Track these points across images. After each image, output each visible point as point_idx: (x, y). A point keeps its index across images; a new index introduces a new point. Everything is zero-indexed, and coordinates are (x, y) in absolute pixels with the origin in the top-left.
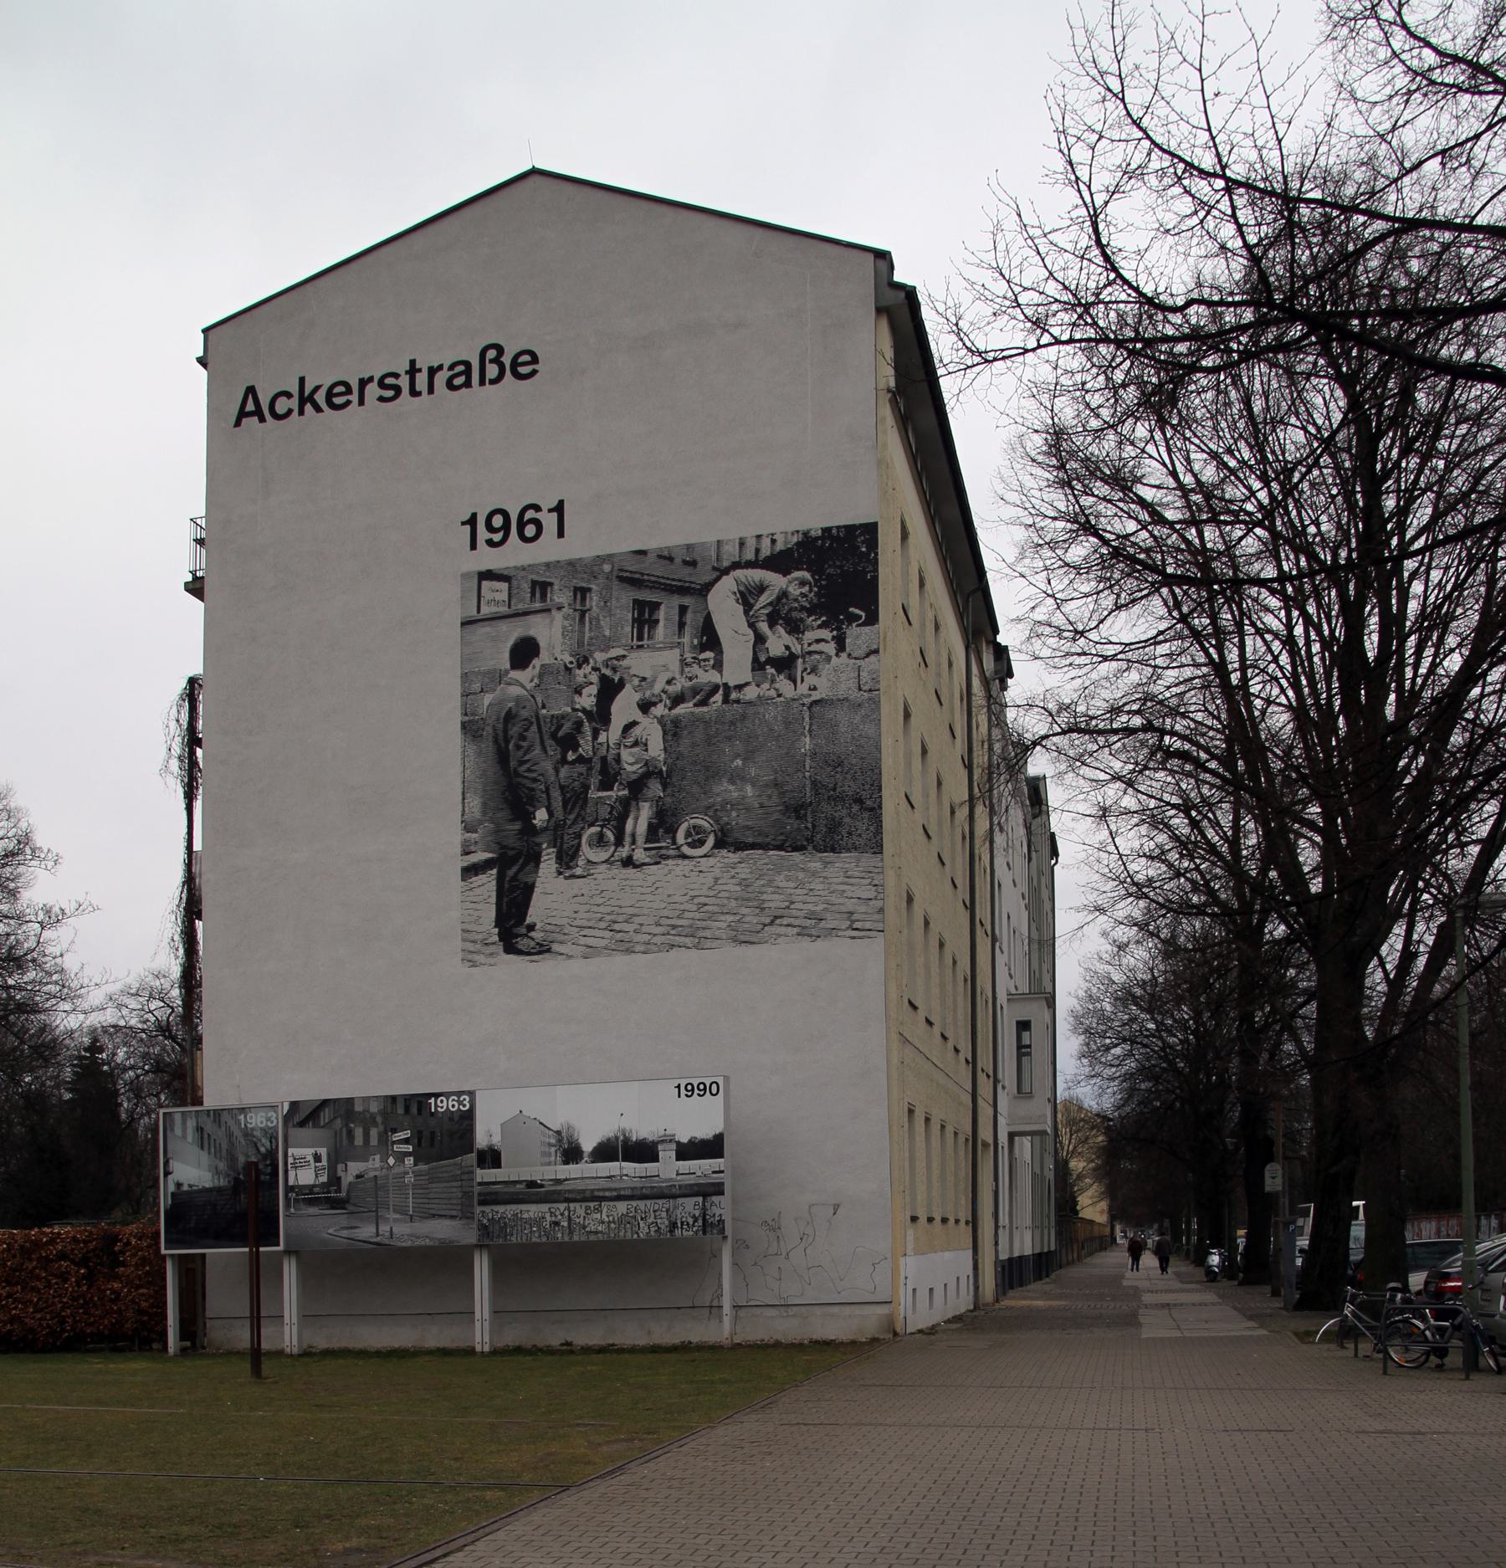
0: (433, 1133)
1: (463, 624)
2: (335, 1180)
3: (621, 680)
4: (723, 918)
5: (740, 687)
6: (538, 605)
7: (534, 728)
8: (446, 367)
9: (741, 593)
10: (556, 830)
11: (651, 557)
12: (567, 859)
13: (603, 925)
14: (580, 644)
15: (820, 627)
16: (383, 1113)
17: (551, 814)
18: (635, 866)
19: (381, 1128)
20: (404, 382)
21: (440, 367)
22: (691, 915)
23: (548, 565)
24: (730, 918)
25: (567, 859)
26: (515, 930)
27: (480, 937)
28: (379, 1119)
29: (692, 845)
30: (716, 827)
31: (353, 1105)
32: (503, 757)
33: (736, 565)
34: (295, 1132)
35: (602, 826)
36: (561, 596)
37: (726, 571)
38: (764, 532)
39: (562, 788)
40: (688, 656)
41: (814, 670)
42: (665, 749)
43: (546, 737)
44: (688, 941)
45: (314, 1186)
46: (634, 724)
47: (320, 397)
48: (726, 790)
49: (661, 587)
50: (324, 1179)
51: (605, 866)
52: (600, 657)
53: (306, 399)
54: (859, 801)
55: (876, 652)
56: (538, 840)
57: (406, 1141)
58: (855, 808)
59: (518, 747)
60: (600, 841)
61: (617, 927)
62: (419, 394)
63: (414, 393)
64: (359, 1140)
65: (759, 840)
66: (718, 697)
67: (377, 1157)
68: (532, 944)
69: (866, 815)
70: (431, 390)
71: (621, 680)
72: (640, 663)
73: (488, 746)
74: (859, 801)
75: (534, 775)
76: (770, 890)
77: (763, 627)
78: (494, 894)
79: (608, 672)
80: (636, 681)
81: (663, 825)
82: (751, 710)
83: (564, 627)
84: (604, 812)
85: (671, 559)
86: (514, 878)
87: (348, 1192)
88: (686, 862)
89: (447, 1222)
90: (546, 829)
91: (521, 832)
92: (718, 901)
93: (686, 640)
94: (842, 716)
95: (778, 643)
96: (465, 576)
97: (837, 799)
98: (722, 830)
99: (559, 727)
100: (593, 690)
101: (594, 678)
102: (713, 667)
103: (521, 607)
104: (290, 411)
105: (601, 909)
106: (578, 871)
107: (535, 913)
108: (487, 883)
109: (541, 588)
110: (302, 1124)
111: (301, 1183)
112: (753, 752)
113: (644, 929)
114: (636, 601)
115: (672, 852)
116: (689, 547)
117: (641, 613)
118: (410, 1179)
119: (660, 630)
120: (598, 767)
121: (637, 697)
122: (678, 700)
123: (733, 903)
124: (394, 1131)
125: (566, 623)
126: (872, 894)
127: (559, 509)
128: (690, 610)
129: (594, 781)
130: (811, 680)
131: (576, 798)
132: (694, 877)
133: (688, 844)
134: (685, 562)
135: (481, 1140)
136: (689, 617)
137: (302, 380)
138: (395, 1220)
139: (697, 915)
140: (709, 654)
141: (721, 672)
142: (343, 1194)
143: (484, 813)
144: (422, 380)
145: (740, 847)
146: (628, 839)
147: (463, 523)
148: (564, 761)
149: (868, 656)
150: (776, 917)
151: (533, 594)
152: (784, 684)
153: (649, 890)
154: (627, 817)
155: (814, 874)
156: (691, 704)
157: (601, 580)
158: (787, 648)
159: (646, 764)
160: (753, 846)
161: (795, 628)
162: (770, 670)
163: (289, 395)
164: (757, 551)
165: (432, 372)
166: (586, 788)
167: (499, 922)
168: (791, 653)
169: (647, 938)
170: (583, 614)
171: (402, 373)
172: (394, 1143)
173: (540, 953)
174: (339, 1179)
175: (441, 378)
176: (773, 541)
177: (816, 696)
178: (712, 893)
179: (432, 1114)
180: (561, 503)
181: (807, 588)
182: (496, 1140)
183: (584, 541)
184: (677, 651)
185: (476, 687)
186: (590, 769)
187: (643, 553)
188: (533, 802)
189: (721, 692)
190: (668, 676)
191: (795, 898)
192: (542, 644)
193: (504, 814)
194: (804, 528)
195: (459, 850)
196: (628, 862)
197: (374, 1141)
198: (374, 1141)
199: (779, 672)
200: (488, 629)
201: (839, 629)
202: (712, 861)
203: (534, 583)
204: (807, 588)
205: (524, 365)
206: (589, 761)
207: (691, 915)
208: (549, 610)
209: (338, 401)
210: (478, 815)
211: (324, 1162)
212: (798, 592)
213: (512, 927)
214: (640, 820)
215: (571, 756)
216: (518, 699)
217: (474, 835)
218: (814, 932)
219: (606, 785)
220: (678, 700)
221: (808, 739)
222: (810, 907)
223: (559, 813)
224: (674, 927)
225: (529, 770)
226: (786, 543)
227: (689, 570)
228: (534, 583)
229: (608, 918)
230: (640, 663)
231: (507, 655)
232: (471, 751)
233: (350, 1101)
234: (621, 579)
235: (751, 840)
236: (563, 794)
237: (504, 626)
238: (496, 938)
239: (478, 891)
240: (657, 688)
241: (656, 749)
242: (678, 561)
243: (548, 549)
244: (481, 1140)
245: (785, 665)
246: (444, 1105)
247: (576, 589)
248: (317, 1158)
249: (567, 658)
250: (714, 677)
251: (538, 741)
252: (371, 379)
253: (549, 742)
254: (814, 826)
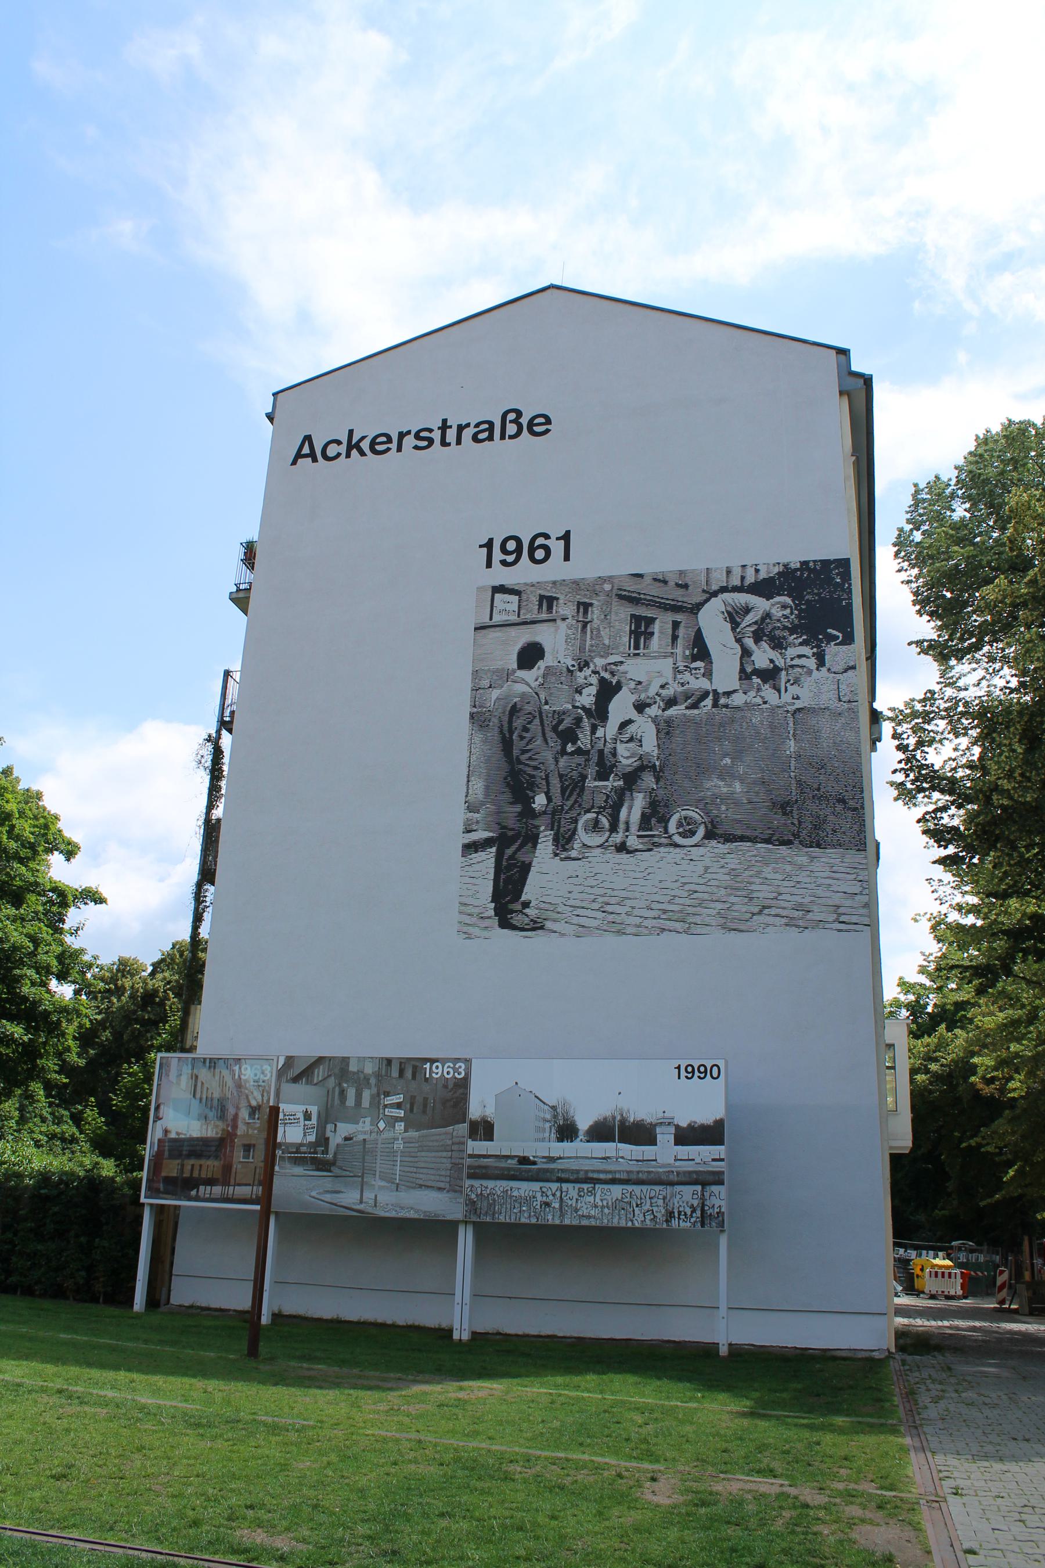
0: (426, 1099)
1: (476, 629)
2: (323, 1141)
3: (619, 683)
4: (712, 905)
5: (728, 694)
6: (544, 616)
7: (537, 721)
8: (472, 425)
9: (729, 613)
10: (554, 814)
11: (648, 580)
12: (563, 842)
13: (596, 906)
14: (582, 649)
15: (801, 644)
16: (378, 1075)
17: (549, 799)
18: (629, 852)
19: (374, 1090)
20: (436, 435)
21: (468, 425)
22: (681, 901)
23: (554, 583)
24: (719, 906)
25: (563, 842)
26: (511, 906)
27: (477, 910)
28: (373, 1081)
29: (683, 835)
30: (706, 819)
31: (348, 1065)
32: (507, 745)
33: (724, 590)
34: (288, 1088)
35: (598, 813)
36: (565, 608)
37: (715, 594)
38: (749, 563)
39: (561, 776)
40: (681, 665)
41: (796, 682)
42: (659, 745)
43: (548, 729)
44: (678, 926)
45: (302, 1145)
46: (630, 722)
47: (365, 445)
48: (715, 785)
49: (655, 607)
50: (312, 1138)
51: (599, 850)
52: (599, 662)
53: (353, 446)
54: (842, 801)
55: (853, 668)
56: (536, 822)
57: (399, 1106)
58: (839, 807)
59: (522, 738)
60: (596, 826)
61: (609, 908)
62: (449, 444)
63: (444, 443)
64: (350, 1101)
65: (748, 833)
66: (708, 702)
67: (368, 1120)
68: (527, 920)
69: (850, 814)
70: (459, 442)
71: (619, 683)
72: (635, 669)
73: (494, 734)
74: (842, 801)
75: (532, 763)
76: (758, 881)
77: (749, 642)
78: (492, 871)
79: (607, 676)
80: (632, 685)
81: (655, 815)
82: (738, 715)
83: (567, 636)
84: (600, 800)
85: (665, 582)
86: (512, 857)
87: (335, 1154)
88: (678, 850)
89: (434, 1194)
90: (545, 813)
91: (521, 815)
92: (708, 889)
93: (679, 650)
94: (825, 726)
95: (763, 656)
96: (480, 589)
97: (821, 799)
98: (712, 822)
99: (561, 722)
100: (593, 690)
101: (594, 680)
102: (704, 676)
103: (529, 617)
104: (339, 455)
105: (596, 891)
106: (574, 854)
107: (530, 892)
108: (487, 859)
109: (548, 602)
110: (296, 1080)
111: (289, 1140)
112: (741, 752)
113: (636, 912)
114: (633, 616)
115: (663, 841)
116: (681, 573)
117: (638, 626)
118: (399, 1145)
119: (655, 642)
120: (595, 759)
121: (633, 698)
122: (671, 702)
123: (723, 892)
124: (387, 1094)
125: (569, 632)
126: (857, 890)
127: (566, 537)
128: (682, 625)
129: (591, 771)
130: (793, 690)
131: (574, 786)
132: (682, 866)
133: (680, 834)
134: (677, 585)
135: (475, 1112)
136: (681, 632)
137: (351, 432)
138: (381, 1188)
139: (688, 902)
140: (699, 664)
141: (710, 680)
142: (330, 1156)
143: (487, 794)
144: (451, 435)
145: (729, 838)
146: (622, 826)
147: (481, 546)
148: (563, 752)
149: (846, 671)
150: (764, 907)
151: (540, 605)
152: (768, 692)
153: (641, 875)
154: (622, 805)
155: (801, 867)
156: (683, 707)
157: (602, 597)
158: (772, 661)
159: (640, 758)
160: (742, 839)
161: (778, 644)
162: (756, 680)
163: (339, 443)
164: (743, 578)
165: (461, 428)
166: (584, 777)
167: (496, 897)
168: (775, 666)
169: (638, 920)
170: (584, 627)
171: (436, 429)
172: (386, 1106)
173: (533, 929)
174: (328, 1139)
175: (468, 434)
176: (757, 571)
177: (799, 704)
178: (702, 881)
179: (426, 1080)
180: (568, 533)
181: (788, 611)
182: (490, 1112)
183: (585, 566)
184: (670, 660)
185: (485, 683)
186: (587, 760)
187: (640, 576)
188: (532, 786)
189: (711, 697)
190: (662, 681)
191: (782, 890)
192: (547, 649)
193: (508, 796)
194: (786, 561)
195: (461, 828)
196: (622, 848)
197: (366, 1102)
198: (366, 1102)
199: (765, 682)
200: (499, 634)
201: (818, 646)
202: (701, 850)
203: (542, 598)
204: (788, 611)
205: (538, 426)
206: (587, 752)
207: (681, 901)
208: (555, 620)
210: (481, 797)
211: (314, 1120)
212: (780, 614)
213: (508, 901)
214: (634, 809)
215: (570, 748)
216: (523, 695)
217: (476, 815)
218: (801, 923)
219: (602, 776)
220: (671, 702)
221: (792, 743)
222: (798, 899)
223: (557, 800)
224: (665, 911)
225: (530, 758)
226: (768, 572)
227: (681, 591)
228: (542, 598)
229: (600, 900)
230: (635, 669)
231: (515, 657)
232: (478, 738)
233: (345, 1060)
234: (621, 597)
235: (739, 833)
236: (561, 781)
237: (513, 631)
238: (492, 913)
239: (476, 867)
240: (652, 692)
241: (650, 745)
242: (672, 583)
243: (555, 570)
244: (475, 1112)
245: (769, 675)
246: (438, 1072)
247: (579, 604)
248: (307, 1116)
249: (570, 662)
250: (704, 684)
251: (540, 734)
252: (409, 433)
253: (550, 734)
254: (800, 822)
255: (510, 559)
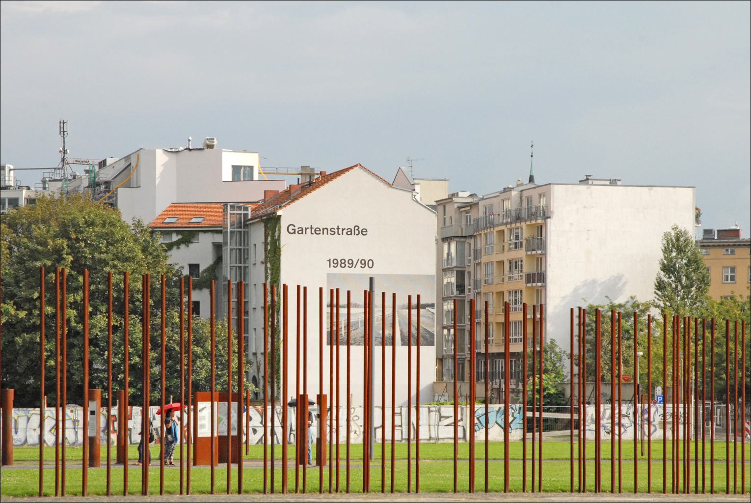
20: (336, 231)
63: (339, 234)
165: (343, 230)
175: (345, 231)
205: (364, 232)
209: (317, 232)
255: (335, 265)
